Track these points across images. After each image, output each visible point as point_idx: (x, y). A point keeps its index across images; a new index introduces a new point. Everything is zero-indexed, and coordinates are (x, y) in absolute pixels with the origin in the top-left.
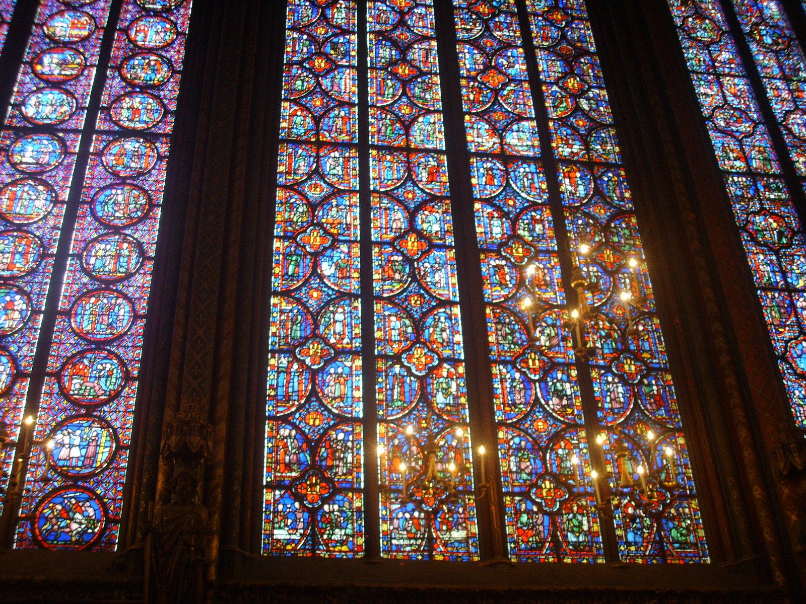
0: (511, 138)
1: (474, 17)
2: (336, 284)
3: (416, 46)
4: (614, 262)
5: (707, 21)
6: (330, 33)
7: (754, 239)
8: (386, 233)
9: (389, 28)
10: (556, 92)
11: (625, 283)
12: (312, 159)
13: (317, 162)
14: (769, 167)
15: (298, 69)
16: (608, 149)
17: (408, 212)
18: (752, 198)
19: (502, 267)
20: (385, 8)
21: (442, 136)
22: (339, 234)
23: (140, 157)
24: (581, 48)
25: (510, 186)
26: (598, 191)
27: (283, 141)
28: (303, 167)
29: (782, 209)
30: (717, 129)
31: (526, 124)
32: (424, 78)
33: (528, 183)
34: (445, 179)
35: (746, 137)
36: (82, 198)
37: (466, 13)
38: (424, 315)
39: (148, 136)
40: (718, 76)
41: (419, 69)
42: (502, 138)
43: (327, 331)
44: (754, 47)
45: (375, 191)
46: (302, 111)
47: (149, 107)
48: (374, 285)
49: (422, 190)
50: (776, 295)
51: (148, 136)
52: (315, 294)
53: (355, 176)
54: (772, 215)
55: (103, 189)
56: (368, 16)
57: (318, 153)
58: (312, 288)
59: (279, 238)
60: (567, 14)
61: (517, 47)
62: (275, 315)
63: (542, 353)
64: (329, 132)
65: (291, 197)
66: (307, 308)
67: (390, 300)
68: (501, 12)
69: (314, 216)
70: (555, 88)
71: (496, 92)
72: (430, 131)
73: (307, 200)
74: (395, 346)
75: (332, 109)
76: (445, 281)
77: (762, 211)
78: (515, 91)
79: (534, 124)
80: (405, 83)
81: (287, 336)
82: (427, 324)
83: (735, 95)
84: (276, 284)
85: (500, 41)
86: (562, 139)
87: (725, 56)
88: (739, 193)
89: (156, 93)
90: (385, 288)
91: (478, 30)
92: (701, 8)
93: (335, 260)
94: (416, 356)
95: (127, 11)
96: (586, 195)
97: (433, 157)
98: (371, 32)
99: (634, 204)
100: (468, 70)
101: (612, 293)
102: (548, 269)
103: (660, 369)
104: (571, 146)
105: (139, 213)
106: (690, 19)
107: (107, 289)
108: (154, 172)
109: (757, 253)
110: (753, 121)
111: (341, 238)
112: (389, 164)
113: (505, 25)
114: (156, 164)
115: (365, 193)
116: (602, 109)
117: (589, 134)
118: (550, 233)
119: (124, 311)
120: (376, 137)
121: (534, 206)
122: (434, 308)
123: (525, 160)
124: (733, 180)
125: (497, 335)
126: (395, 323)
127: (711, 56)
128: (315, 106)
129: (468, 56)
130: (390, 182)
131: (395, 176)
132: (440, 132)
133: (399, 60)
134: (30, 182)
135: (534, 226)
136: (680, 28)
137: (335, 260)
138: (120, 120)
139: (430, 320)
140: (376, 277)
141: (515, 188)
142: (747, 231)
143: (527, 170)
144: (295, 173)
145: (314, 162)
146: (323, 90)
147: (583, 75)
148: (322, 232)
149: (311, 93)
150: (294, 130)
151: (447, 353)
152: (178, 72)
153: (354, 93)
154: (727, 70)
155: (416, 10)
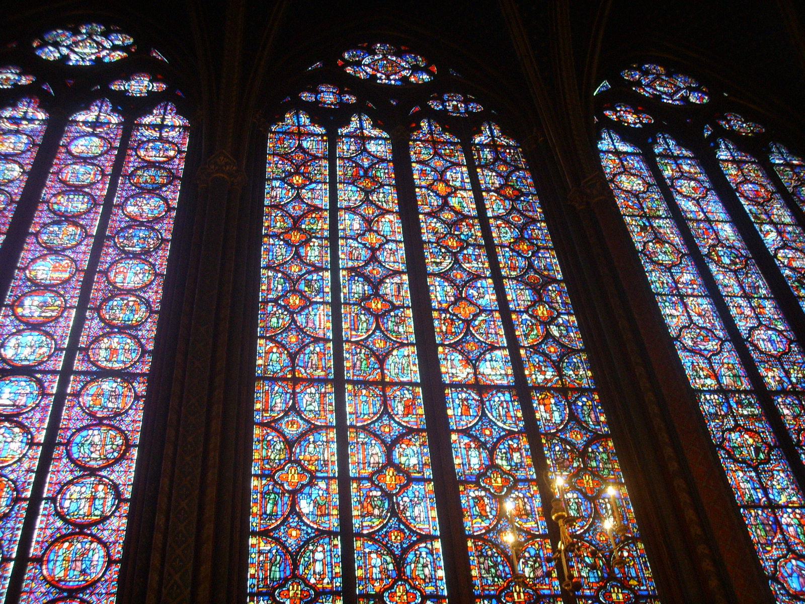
0: (485, 368)
1: (443, 250)
2: (315, 522)
3: (387, 281)
4: (594, 488)
5: (667, 245)
6: (304, 271)
7: (731, 456)
8: (364, 469)
9: (361, 264)
10: (526, 320)
11: (606, 508)
12: (288, 396)
13: (294, 399)
14: (739, 384)
15: (273, 306)
16: (580, 374)
17: (386, 446)
18: (726, 415)
19: (482, 498)
20: (356, 245)
21: (416, 368)
22: (317, 471)
23: (117, 397)
24: (548, 276)
25: (486, 415)
26: (573, 417)
27: (260, 378)
28: (279, 403)
29: (757, 424)
30: (685, 348)
31: (498, 353)
32: (397, 311)
33: (504, 412)
34: (421, 411)
35: (714, 355)
36: (58, 439)
37: (435, 247)
38: (405, 551)
39: (125, 376)
41: (391, 303)
42: (475, 368)
43: (307, 571)
44: (713, 268)
45: (352, 426)
46: (278, 348)
47: (127, 347)
48: (354, 521)
49: (399, 424)
50: (760, 512)
51: (125, 376)
52: (294, 533)
53: (331, 411)
54: (748, 431)
55: (79, 430)
56: (340, 253)
57: (294, 390)
58: (290, 527)
59: (257, 476)
60: (532, 244)
61: (486, 278)
62: (253, 556)
63: (526, 585)
64: (305, 368)
65: (268, 434)
66: (287, 548)
67: (370, 537)
68: (468, 245)
69: (291, 452)
70: (525, 316)
71: (468, 323)
72: (404, 364)
73: (284, 436)
74: (376, 584)
75: (308, 345)
76: (424, 515)
77: (736, 428)
78: (486, 320)
79: (506, 352)
80: (378, 317)
81: (266, 578)
82: (409, 560)
83: (699, 315)
84: (254, 524)
85: (469, 273)
86: (534, 366)
87: (686, 277)
88: (712, 411)
89: (134, 333)
90: (365, 524)
91: (447, 263)
92: (661, 233)
93: (313, 498)
94: (399, 594)
95: (107, 254)
96: (562, 421)
97: (408, 390)
98: (343, 269)
99: (609, 428)
100: (440, 303)
101: (594, 519)
102: (528, 498)
103: (648, 596)
104: (544, 373)
105: (116, 454)
106: (651, 244)
107: (81, 533)
108: (130, 412)
109: (737, 470)
110: (719, 339)
111: (319, 474)
112: (365, 399)
113: (474, 257)
114: (133, 404)
115: (342, 428)
116: (572, 334)
117: (561, 360)
118: (529, 461)
119: (98, 556)
120: (351, 371)
121: (510, 434)
122: (415, 543)
123: (499, 388)
124: (706, 399)
125: (480, 568)
126: (375, 560)
127: (673, 278)
128: (290, 343)
129: (438, 288)
130: (366, 417)
131: (371, 411)
132: (414, 364)
133: (371, 295)
134: (7, 424)
135: (512, 455)
136: (641, 252)
137: (313, 498)
138: (98, 361)
139: (411, 556)
140: (355, 513)
141: (491, 417)
142: (724, 448)
143: (502, 399)
144: (272, 410)
145: (290, 398)
146: (298, 327)
147: (552, 302)
148: (299, 469)
149: (287, 329)
150: (270, 367)
151: (430, 589)
152: (156, 312)
153: (328, 329)
154: (690, 291)
155: (386, 246)
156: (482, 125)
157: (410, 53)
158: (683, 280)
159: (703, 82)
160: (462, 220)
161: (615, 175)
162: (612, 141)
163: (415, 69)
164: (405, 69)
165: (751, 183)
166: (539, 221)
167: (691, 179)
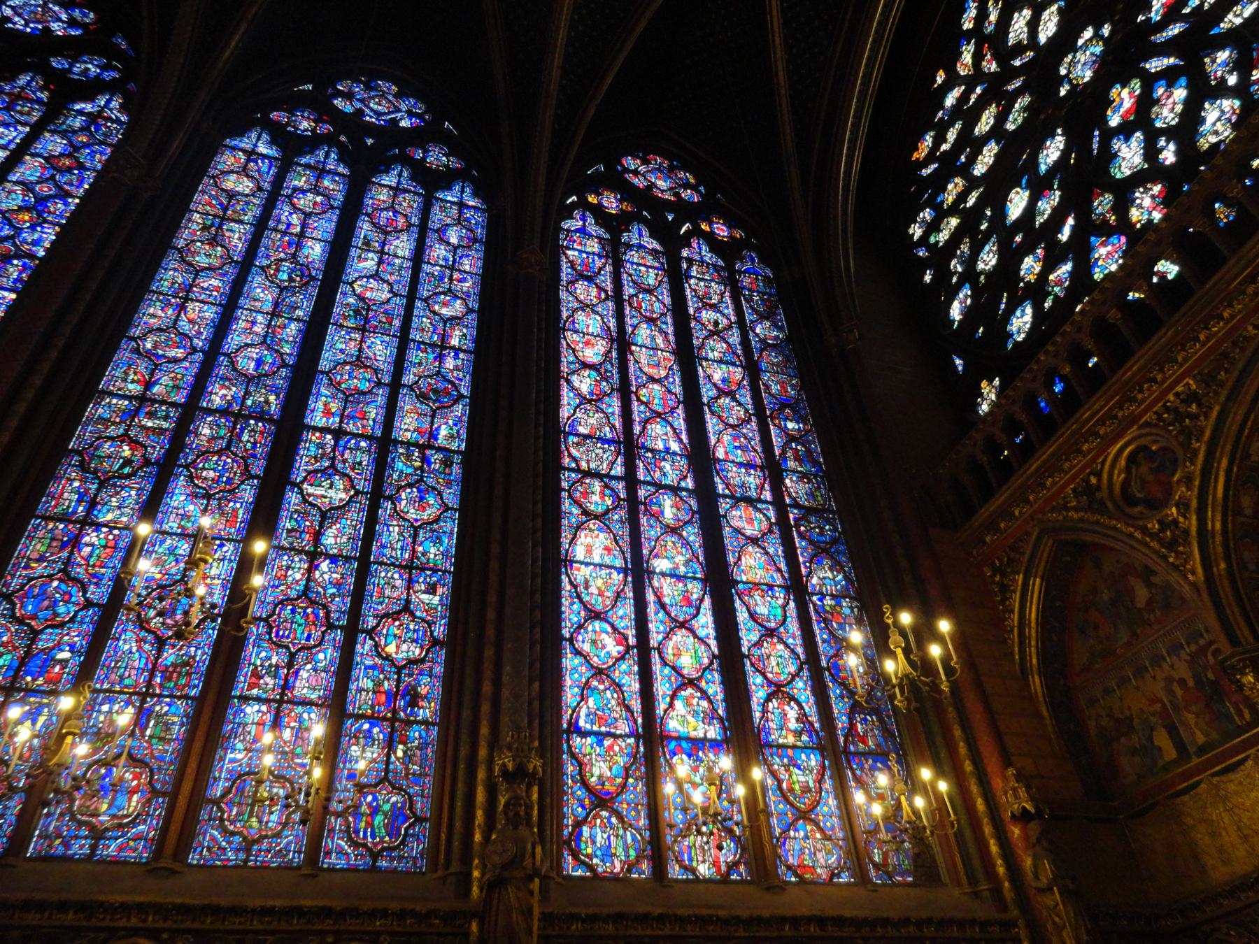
7: (83, 467)
35: (169, 362)
40: (187, 299)
54: (134, 443)
77: (125, 438)
83: (191, 321)
92: (223, 235)
156: (103, 93)
157: (80, 6)
158: (205, 285)
159: (437, 107)
161: (224, 173)
162: (259, 138)
163: (72, 23)
164: (60, 20)
166: (73, 197)
167: (318, 194)
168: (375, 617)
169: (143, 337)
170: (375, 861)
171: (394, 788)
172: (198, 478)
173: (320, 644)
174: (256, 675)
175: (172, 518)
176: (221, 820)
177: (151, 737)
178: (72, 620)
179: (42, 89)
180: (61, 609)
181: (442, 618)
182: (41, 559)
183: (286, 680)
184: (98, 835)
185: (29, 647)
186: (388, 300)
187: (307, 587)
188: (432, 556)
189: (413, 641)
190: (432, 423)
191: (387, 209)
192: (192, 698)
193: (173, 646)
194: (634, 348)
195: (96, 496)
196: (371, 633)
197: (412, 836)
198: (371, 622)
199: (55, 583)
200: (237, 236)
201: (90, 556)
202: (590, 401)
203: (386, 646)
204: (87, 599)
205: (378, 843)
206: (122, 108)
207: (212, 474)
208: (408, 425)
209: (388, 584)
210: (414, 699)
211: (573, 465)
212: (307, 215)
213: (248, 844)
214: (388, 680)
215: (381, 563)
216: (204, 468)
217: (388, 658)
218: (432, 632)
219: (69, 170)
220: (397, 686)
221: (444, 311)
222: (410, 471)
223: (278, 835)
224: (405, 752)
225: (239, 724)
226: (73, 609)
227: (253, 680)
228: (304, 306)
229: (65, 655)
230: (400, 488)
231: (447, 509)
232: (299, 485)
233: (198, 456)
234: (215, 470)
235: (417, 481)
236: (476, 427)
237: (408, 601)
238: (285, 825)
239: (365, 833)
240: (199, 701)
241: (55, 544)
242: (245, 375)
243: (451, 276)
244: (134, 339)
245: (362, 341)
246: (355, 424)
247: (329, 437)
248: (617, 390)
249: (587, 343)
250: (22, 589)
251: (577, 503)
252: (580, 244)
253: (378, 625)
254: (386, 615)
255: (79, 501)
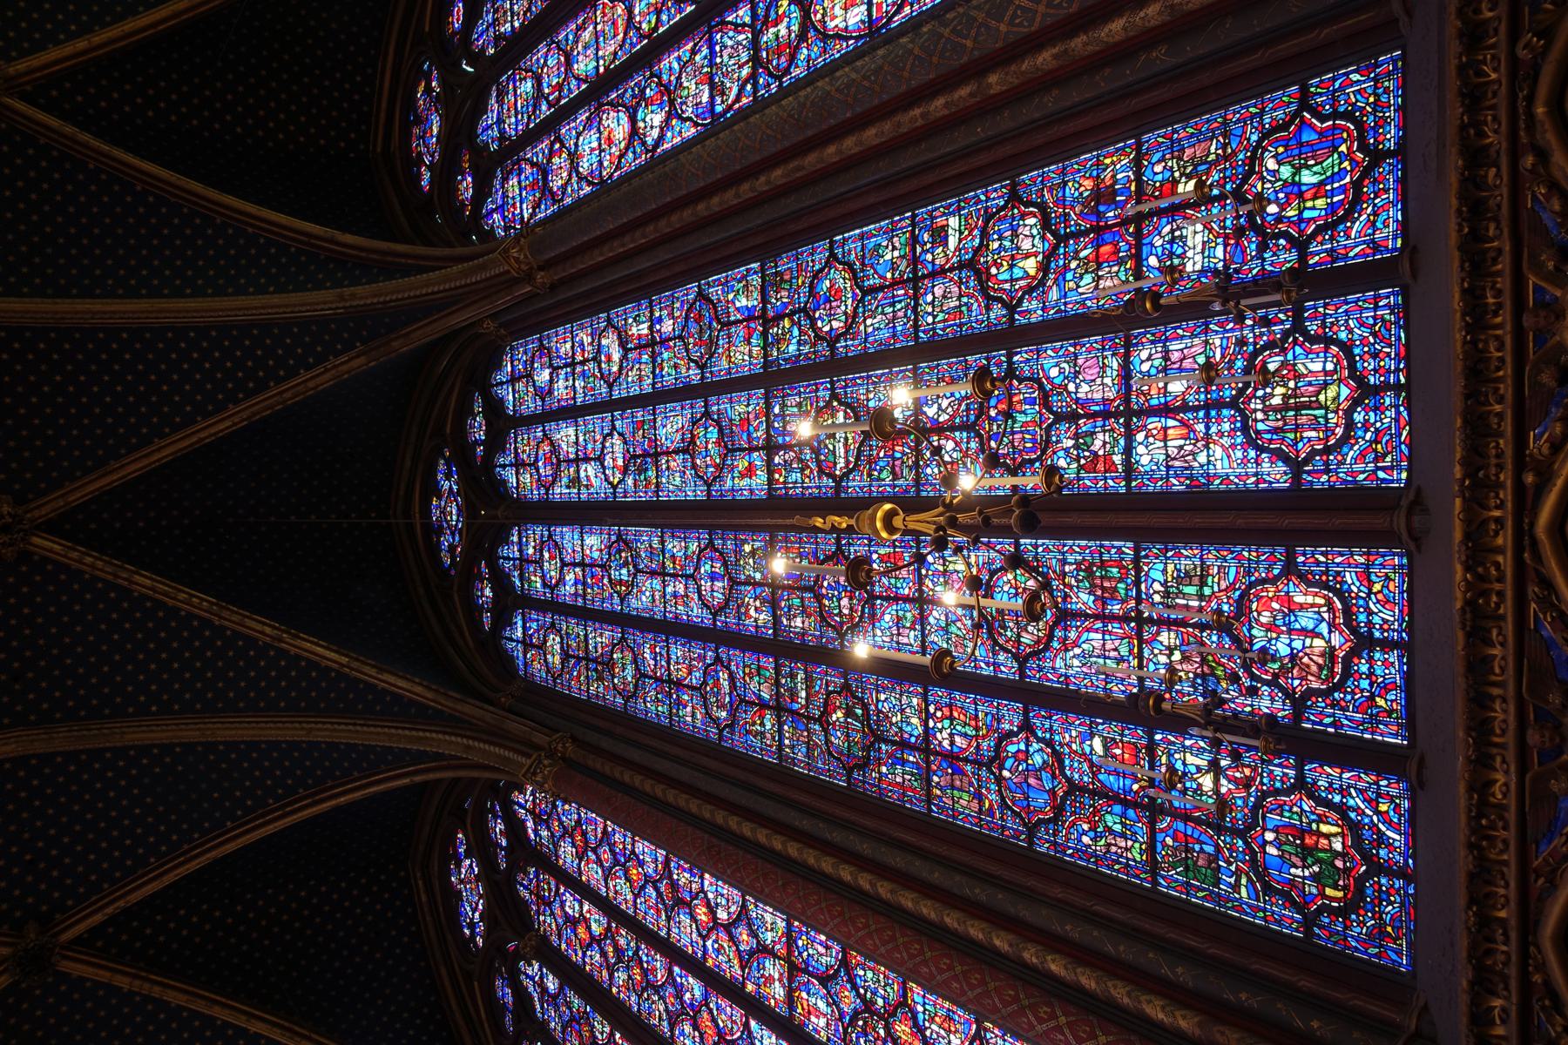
7: (864, 764)
40: (670, 681)
54: (828, 709)
70: (709, 943)
77: (823, 720)
117: (756, 936)
160: (613, 939)
165: (537, 460)
168: (988, 308)
169: (716, 721)
170: (1389, 153)
171: (1251, 172)
172: (852, 618)
173: (1039, 381)
174: (1091, 467)
175: (905, 640)
176: (1327, 450)
177: (1201, 597)
178: (1050, 743)
179: (527, 874)
180: (1038, 760)
181: (980, 201)
182: (978, 796)
183: (1094, 415)
184: (1364, 643)
185: (1093, 793)
186: (621, 434)
187: (963, 427)
188: (896, 253)
189: (1015, 234)
190: (737, 322)
191: (537, 470)
192: (1137, 550)
193: (1066, 597)
194: (602, 70)
195: (894, 743)
196: (1011, 308)
197: (1334, 102)
198: (997, 311)
199: (1006, 774)
200: (601, 639)
201: (965, 735)
202: (672, 102)
203: (1027, 276)
204: (1021, 729)
205: (1352, 160)
206: (522, 791)
207: (845, 602)
208: (743, 355)
209: (944, 303)
210: (1103, 195)
211: (749, 87)
212: (564, 564)
213: (1365, 393)
214: (1077, 252)
215: (916, 326)
216: (840, 614)
217: (1044, 268)
218: (1000, 209)
219: (584, 834)
220: (1086, 233)
221: (616, 357)
222: (796, 332)
223: (1347, 348)
224: (1189, 177)
225: (1168, 467)
226: (1036, 746)
227: (1100, 467)
228: (646, 538)
229: (1097, 743)
230: (819, 337)
231: (833, 255)
232: (838, 480)
233: (829, 625)
234: (839, 600)
235: (808, 316)
236: (726, 259)
237: (961, 266)
238: (1328, 341)
239: (1333, 193)
240: (1140, 536)
241: (958, 783)
242: (731, 588)
243: (583, 363)
244: (721, 731)
245: (667, 453)
246: (756, 429)
247: (777, 460)
248: (651, 68)
249: (610, 141)
250: (1018, 815)
251: (792, 58)
252: (514, 205)
253: (1000, 300)
254: (984, 291)
255: (904, 762)
